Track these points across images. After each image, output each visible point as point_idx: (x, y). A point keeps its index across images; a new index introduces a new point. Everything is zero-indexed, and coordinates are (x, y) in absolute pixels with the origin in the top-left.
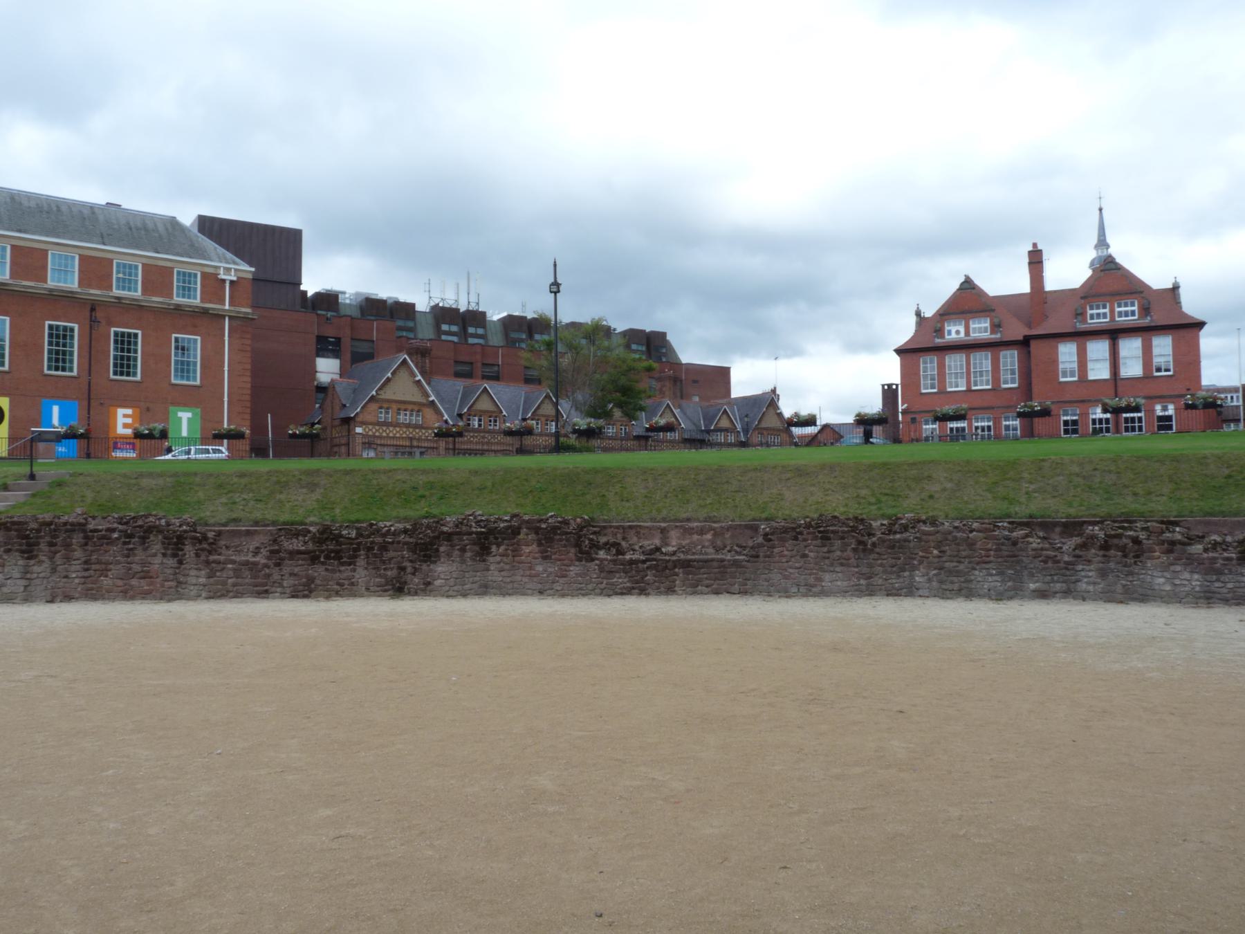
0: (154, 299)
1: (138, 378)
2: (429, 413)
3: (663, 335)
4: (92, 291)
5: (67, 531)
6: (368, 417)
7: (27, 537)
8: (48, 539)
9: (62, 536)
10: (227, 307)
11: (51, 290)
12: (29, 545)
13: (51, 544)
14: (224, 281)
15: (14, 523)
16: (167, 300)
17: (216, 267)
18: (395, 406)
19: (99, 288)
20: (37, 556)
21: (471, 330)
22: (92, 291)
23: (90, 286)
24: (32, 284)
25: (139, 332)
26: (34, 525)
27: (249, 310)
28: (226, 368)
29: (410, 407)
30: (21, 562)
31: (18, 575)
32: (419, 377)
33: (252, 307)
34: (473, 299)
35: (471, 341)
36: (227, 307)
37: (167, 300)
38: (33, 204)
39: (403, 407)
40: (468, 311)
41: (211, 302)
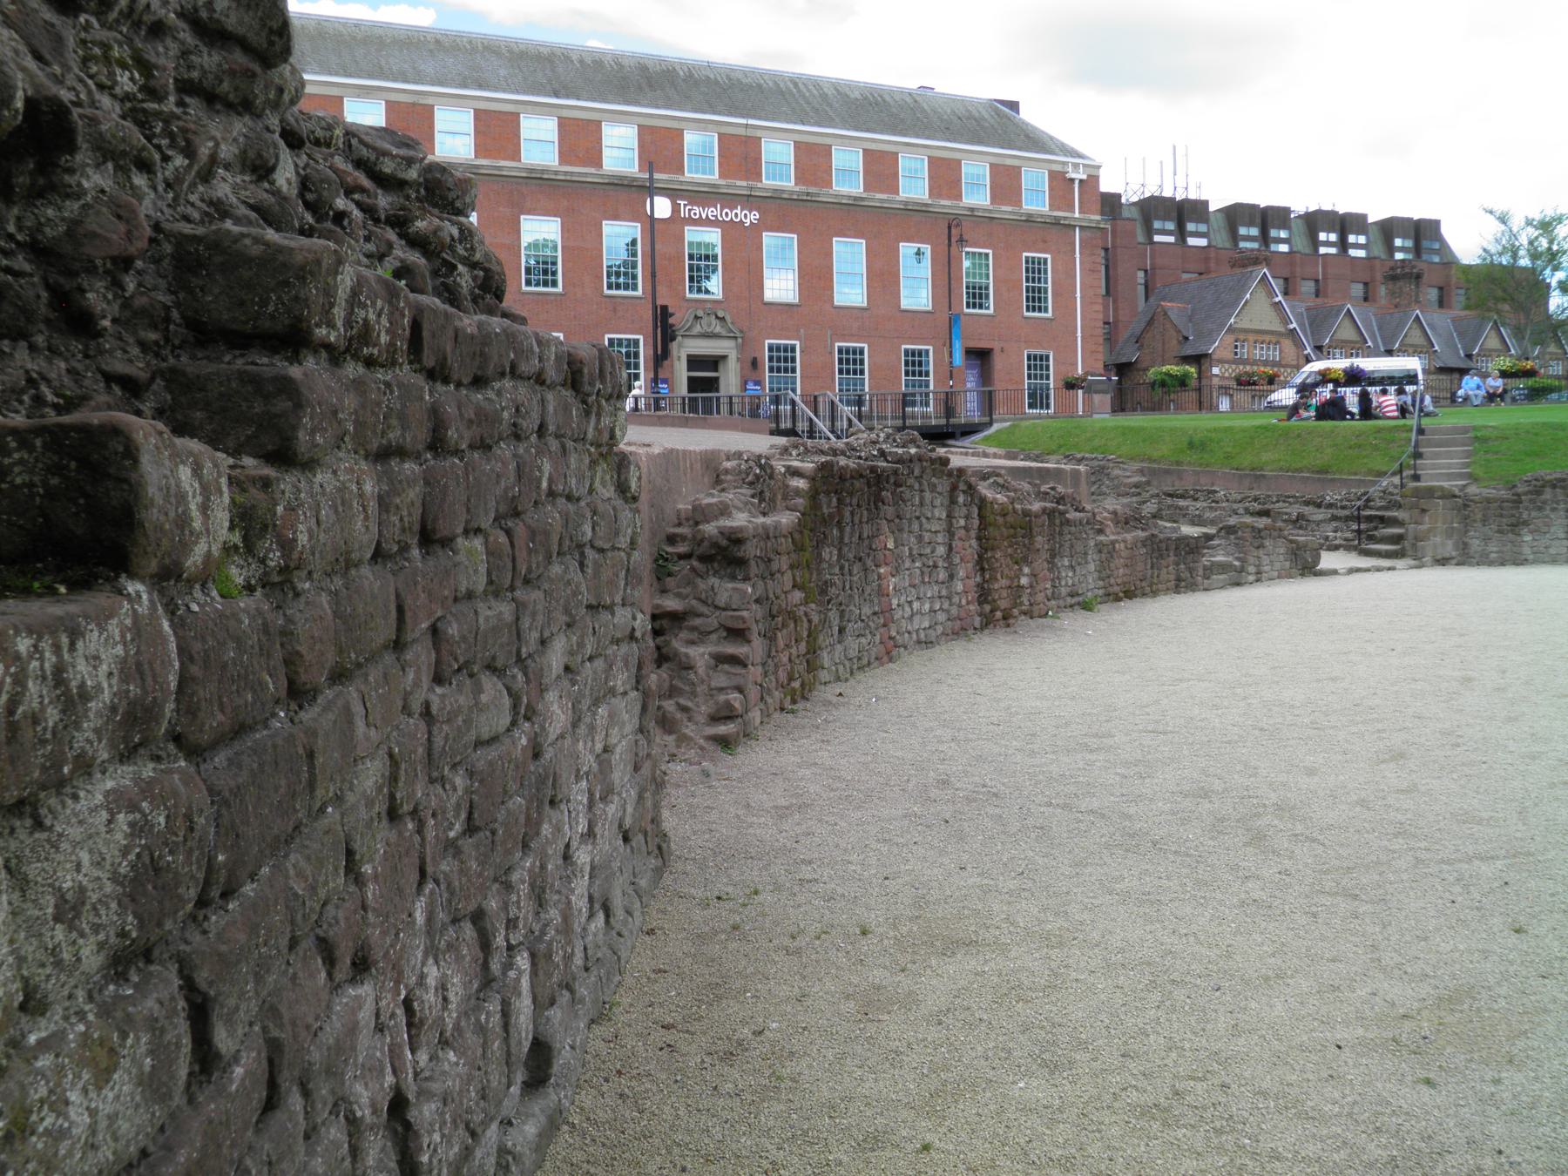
0: (1004, 208)
1: (991, 311)
2: (1287, 344)
3: (1434, 226)
4: (943, 202)
6: (1227, 354)
10: (1077, 215)
11: (906, 203)
14: (1072, 180)
16: (1016, 209)
17: (1064, 163)
18: (1251, 338)
19: (949, 198)
21: (1191, 227)
22: (943, 202)
23: (940, 196)
24: (884, 196)
25: (1048, 256)
27: (1098, 218)
28: (1078, 294)
29: (1267, 338)
32: (1280, 298)
33: (1102, 214)
34: (1181, 184)
35: (1322, 250)
36: (1077, 215)
37: (1016, 209)
38: (856, 94)
39: (1260, 338)
40: (1186, 201)
41: (1059, 209)
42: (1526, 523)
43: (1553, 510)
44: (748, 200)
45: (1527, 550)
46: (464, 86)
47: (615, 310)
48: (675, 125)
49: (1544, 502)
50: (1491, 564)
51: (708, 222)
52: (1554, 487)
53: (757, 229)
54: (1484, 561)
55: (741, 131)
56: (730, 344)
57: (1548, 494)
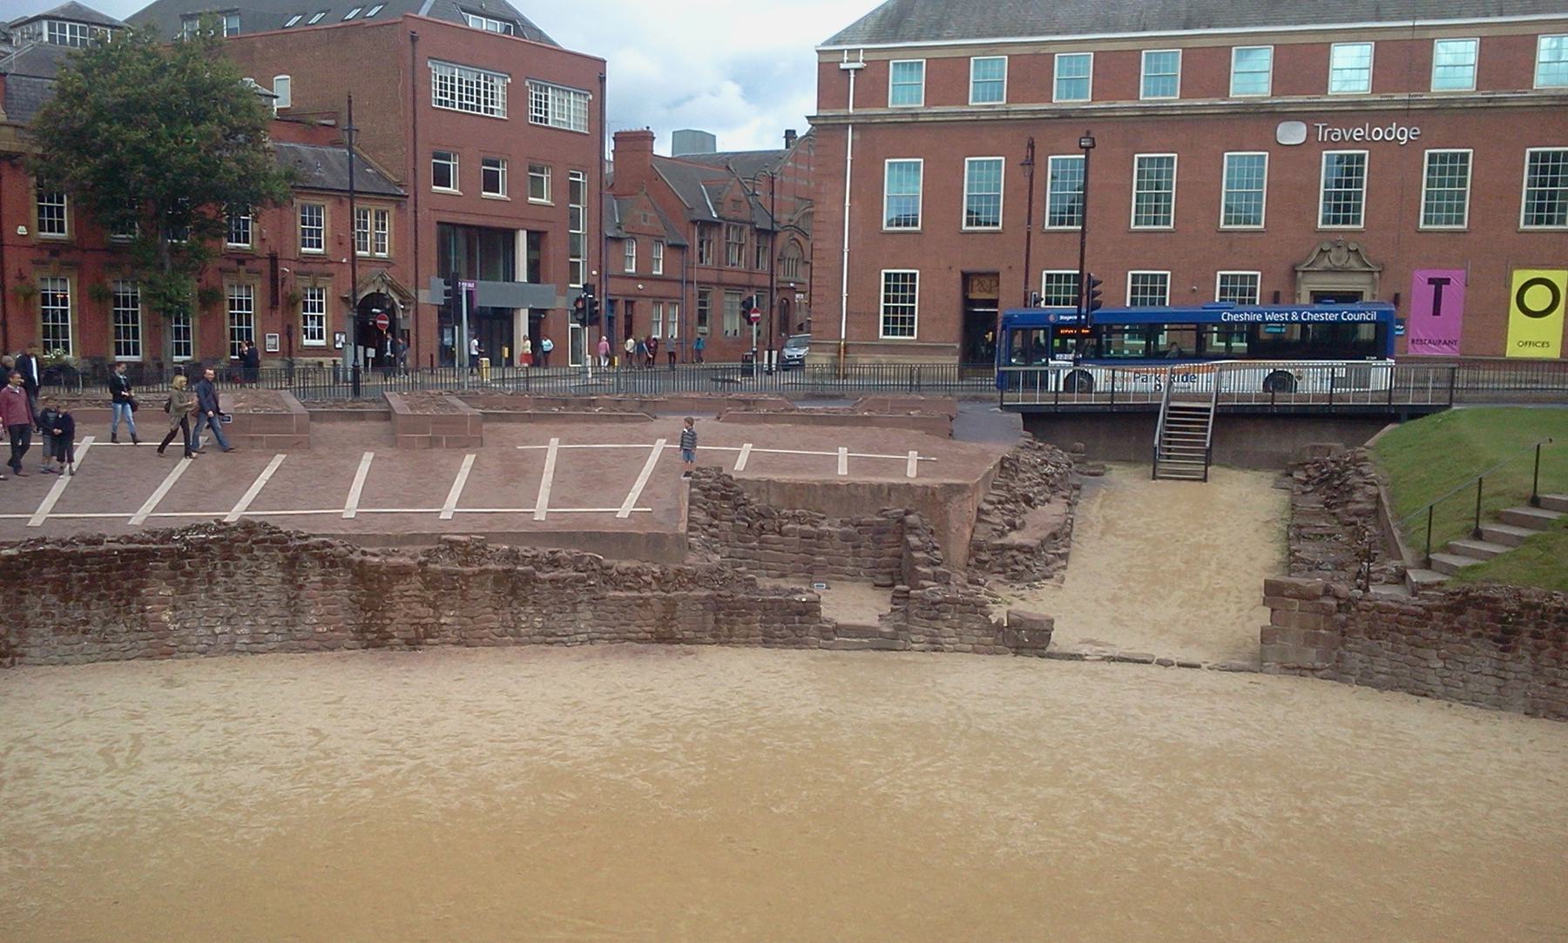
5: (1558, 620)
7: (1504, 621)
8: (1532, 627)
9: (1552, 626)
12: (1504, 631)
13: (1535, 635)
15: (1487, 599)
20: (1515, 649)
26: (1514, 606)
30: (1494, 654)
31: (1488, 671)
42: (1435, 645)
43: (1478, 635)
44: (1406, 115)
45: (1433, 679)
46: (1088, 31)
47: (1230, 245)
48: (1319, 39)
49: (1464, 625)
50: (1376, 686)
51: (1353, 144)
52: (1479, 606)
53: (1415, 146)
54: (1366, 679)
55: (1407, 35)
56: (1365, 279)
57: (1470, 615)
